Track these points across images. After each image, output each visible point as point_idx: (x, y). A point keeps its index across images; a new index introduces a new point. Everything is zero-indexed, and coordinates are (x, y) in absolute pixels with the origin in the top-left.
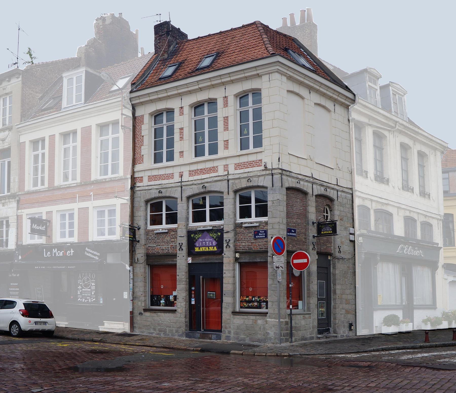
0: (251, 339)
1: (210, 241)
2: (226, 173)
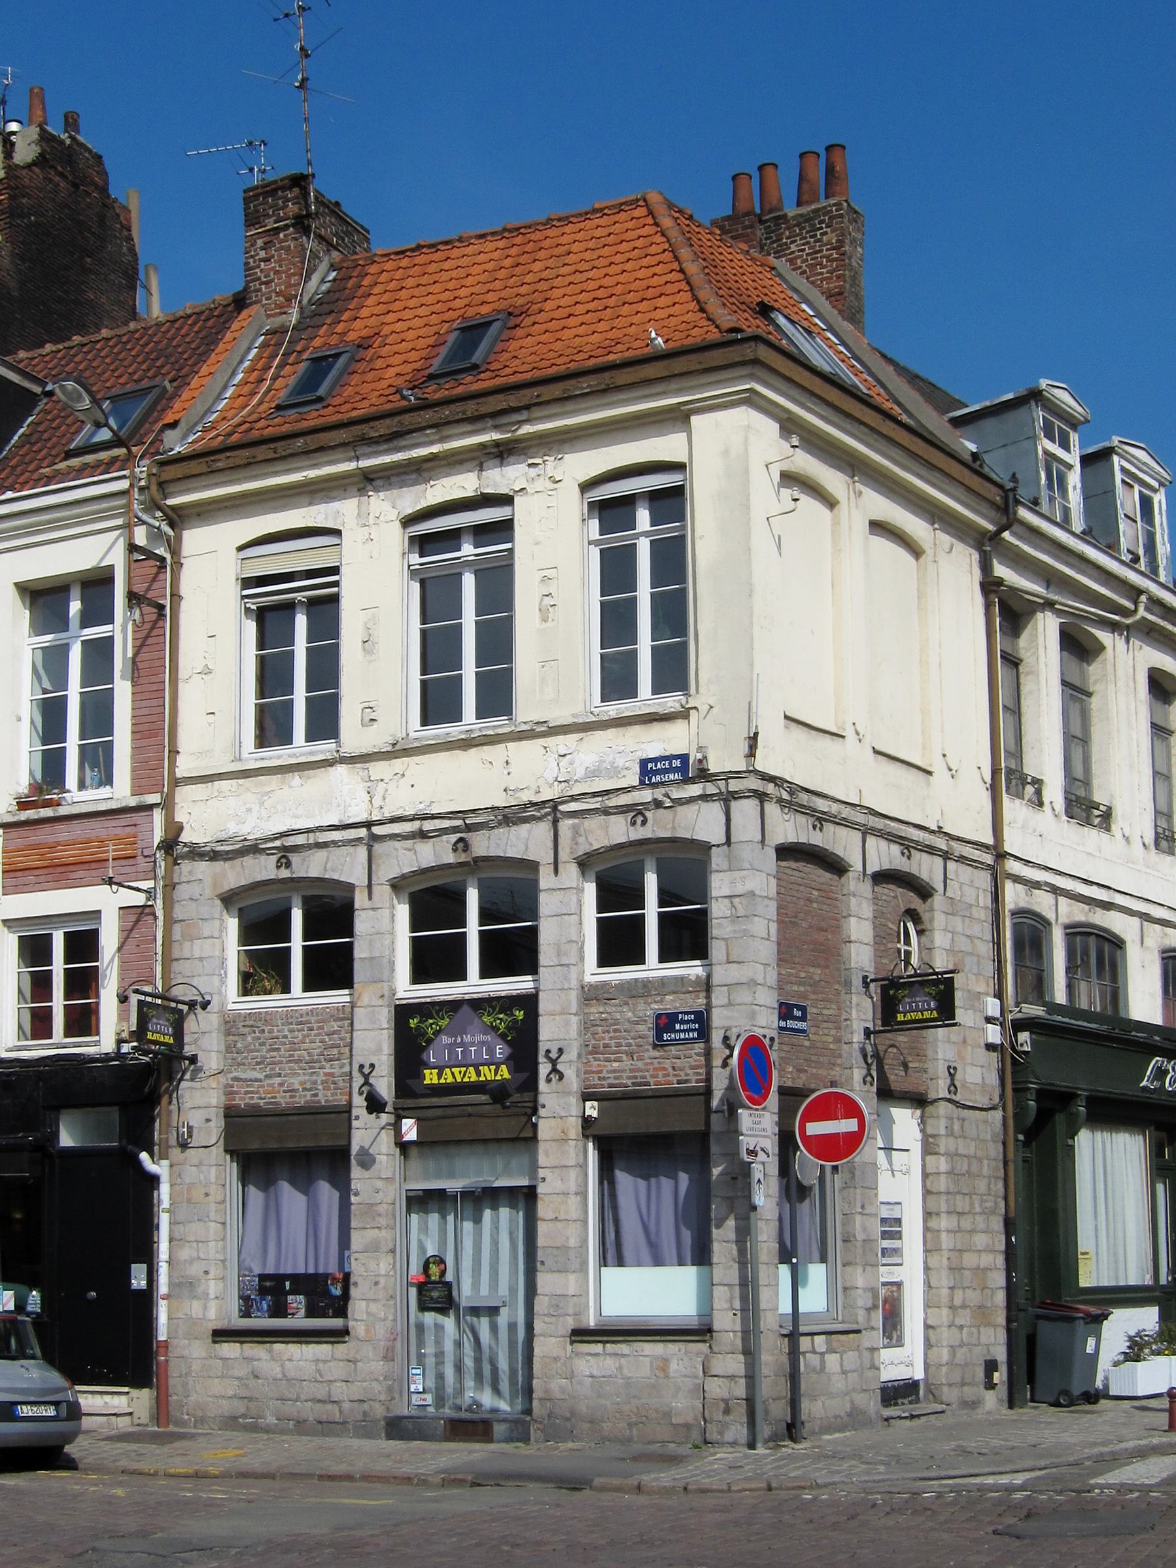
1: (483, 1043)
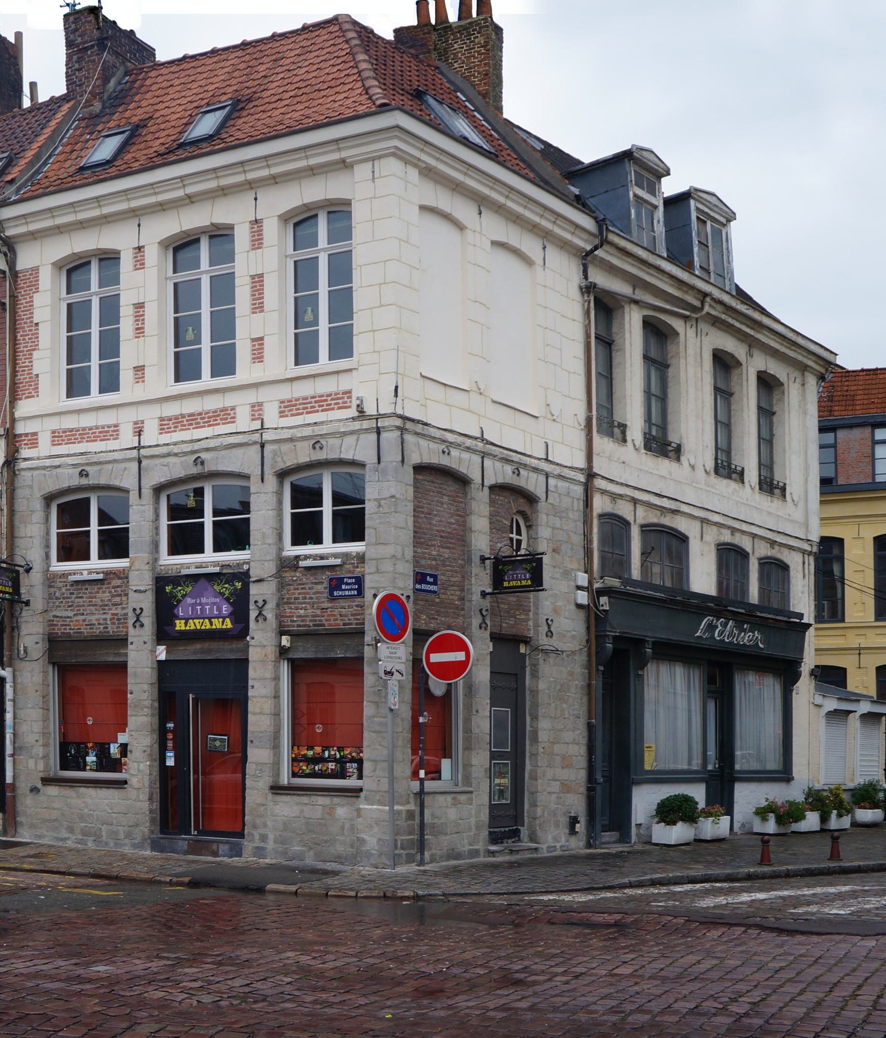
0: (318, 856)
1: (214, 604)
2: (257, 425)
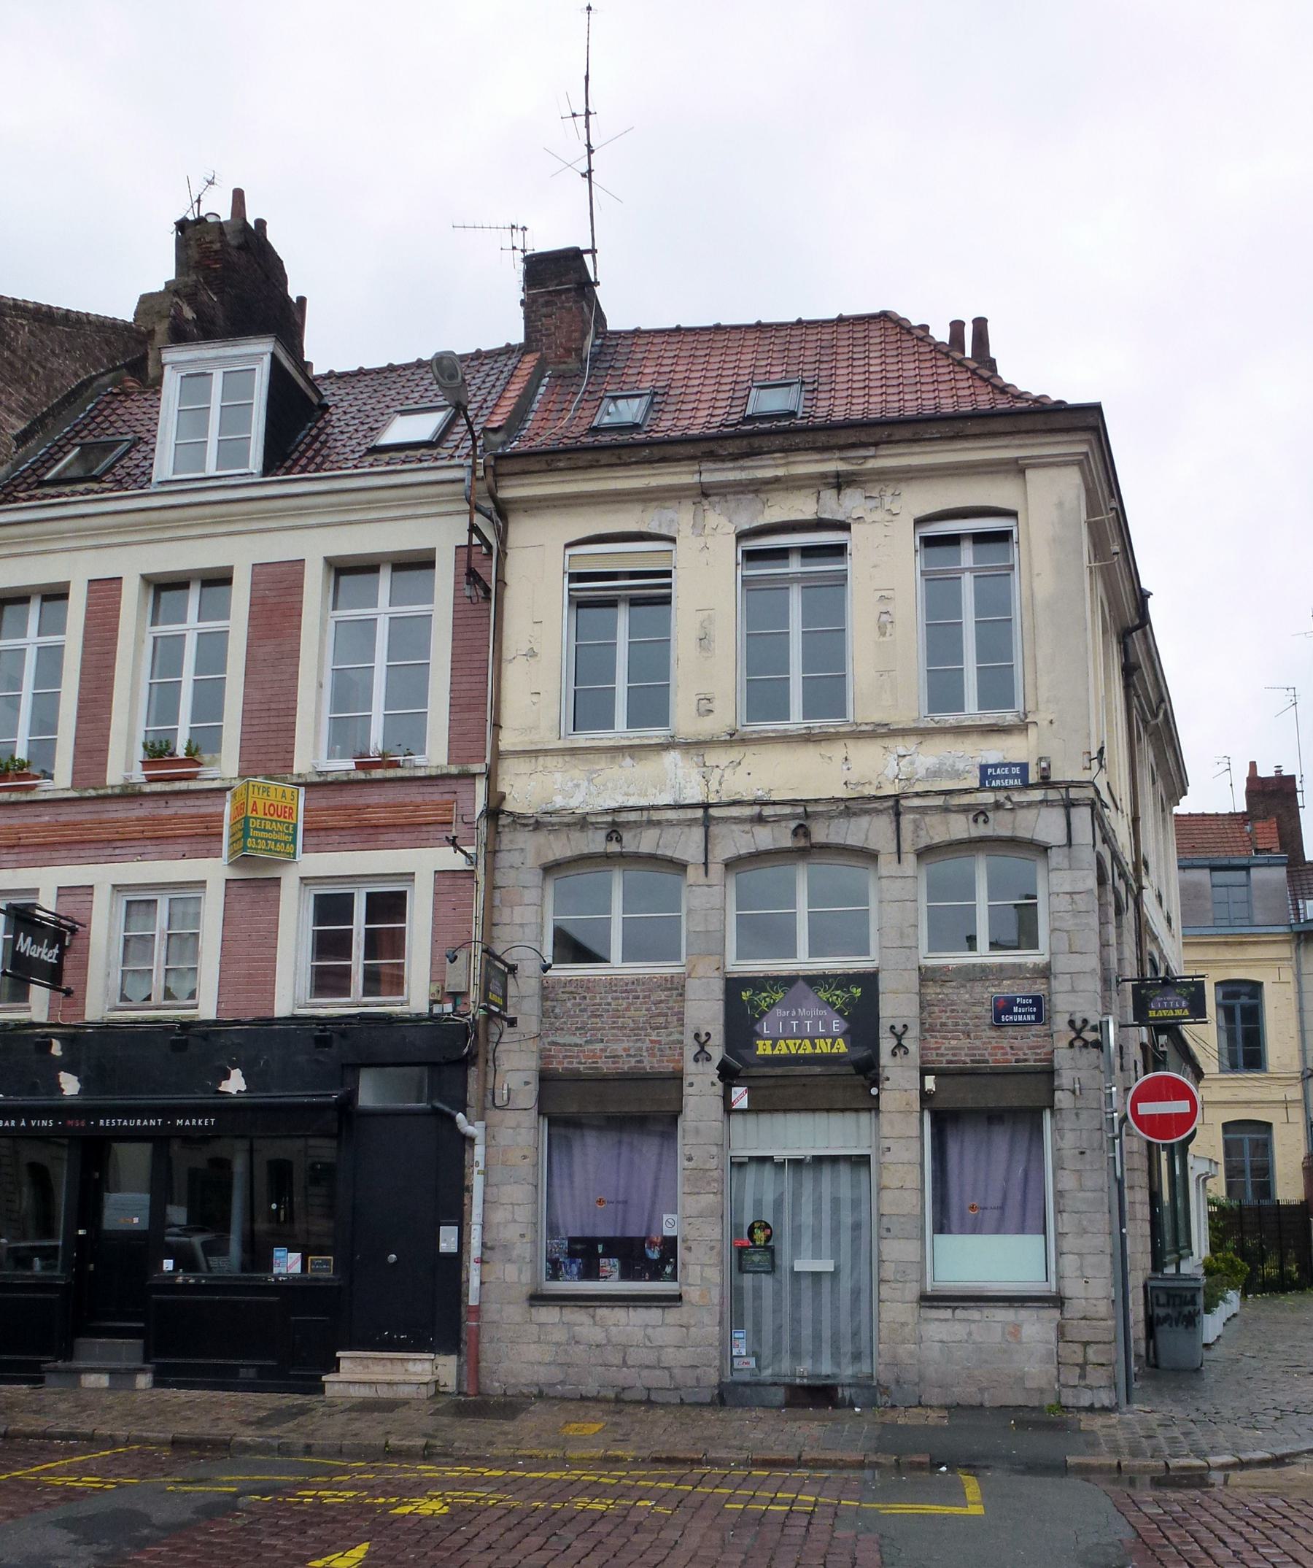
1: (820, 1017)
